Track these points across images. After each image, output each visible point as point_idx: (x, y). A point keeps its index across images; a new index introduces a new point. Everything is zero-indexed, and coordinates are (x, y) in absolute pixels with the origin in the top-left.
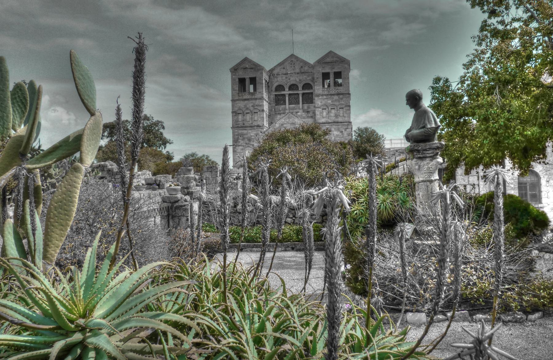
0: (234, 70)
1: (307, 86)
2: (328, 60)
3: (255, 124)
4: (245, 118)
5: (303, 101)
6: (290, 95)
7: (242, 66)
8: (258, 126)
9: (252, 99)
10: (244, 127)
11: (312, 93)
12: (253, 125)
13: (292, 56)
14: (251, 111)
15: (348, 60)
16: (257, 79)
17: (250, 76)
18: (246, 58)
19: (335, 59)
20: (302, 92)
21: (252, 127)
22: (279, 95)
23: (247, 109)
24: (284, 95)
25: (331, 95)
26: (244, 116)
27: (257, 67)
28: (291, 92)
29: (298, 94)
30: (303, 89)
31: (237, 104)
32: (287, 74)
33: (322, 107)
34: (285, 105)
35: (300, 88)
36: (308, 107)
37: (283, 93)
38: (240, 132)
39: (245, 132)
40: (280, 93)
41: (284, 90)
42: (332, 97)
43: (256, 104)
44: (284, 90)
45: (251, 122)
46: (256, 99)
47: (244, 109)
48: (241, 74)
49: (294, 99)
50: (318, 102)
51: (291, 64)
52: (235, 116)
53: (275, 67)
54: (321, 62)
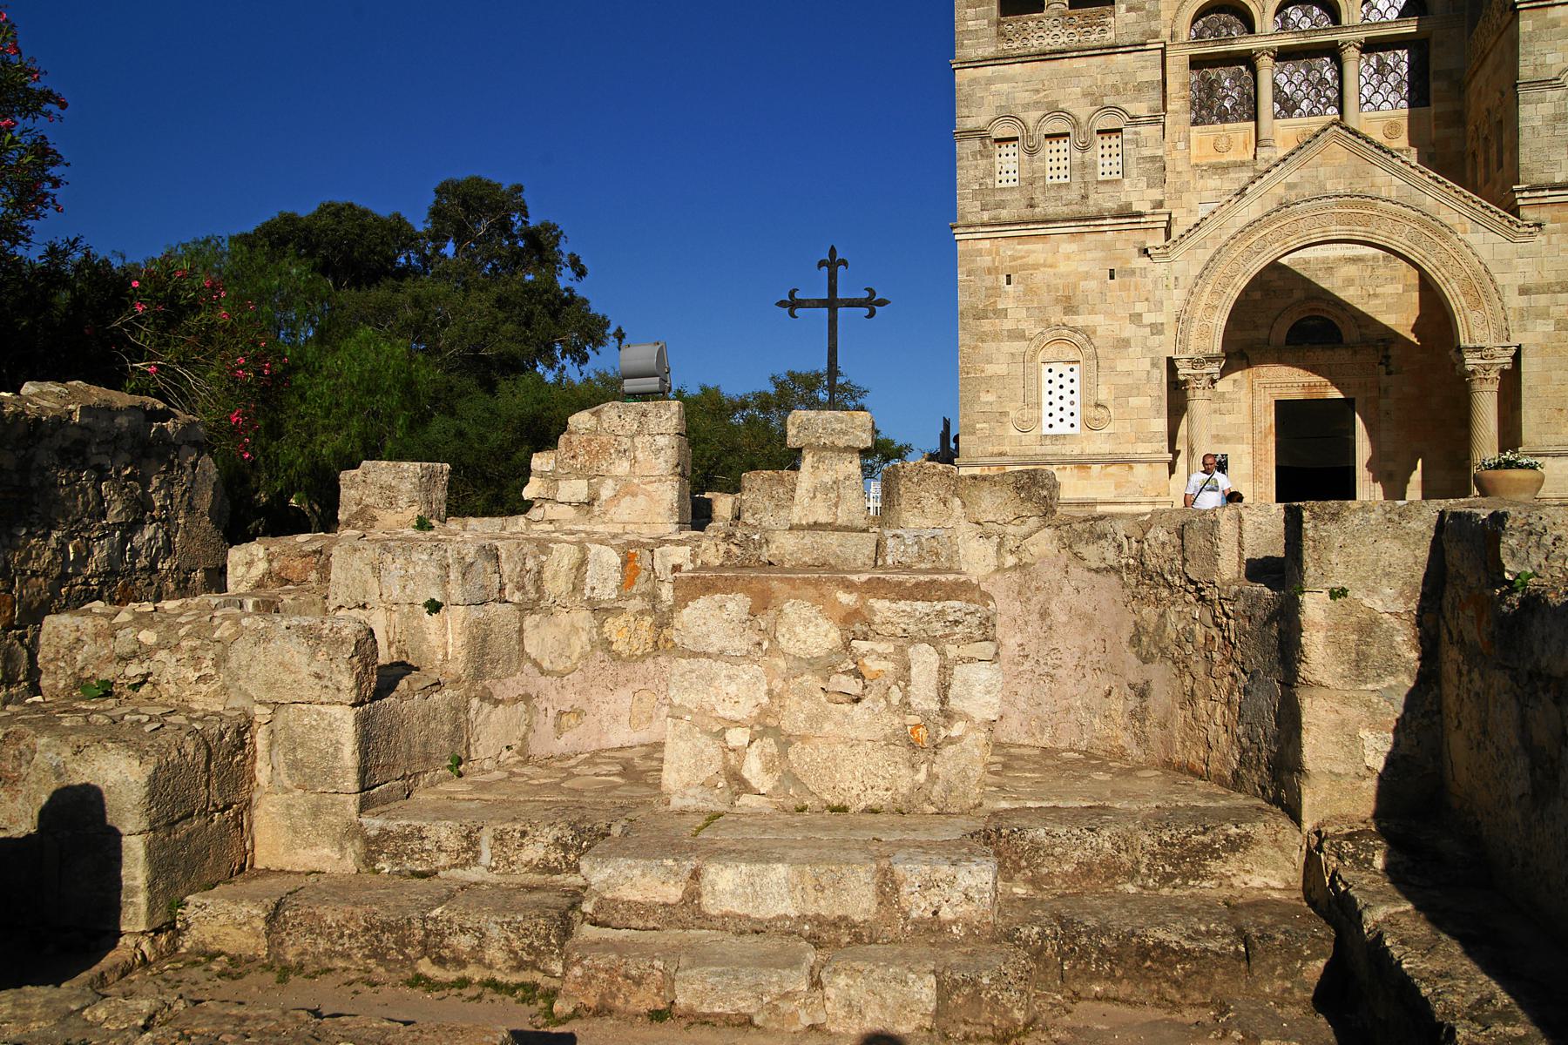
3: (1104, 200)
4: (1037, 164)
8: (1126, 213)
9: (1084, 52)
12: (1093, 210)
14: (1076, 124)
20: (1362, 35)
23: (1055, 111)
26: (1032, 152)
28: (1289, 40)
31: (990, 81)
34: (1255, 117)
37: (1243, 44)
38: (1009, 249)
39: (1036, 252)
40: (1221, 49)
43: (1110, 80)
44: (1250, 27)
45: (1074, 195)
46: (1112, 49)
47: (1031, 117)
52: (985, 154)
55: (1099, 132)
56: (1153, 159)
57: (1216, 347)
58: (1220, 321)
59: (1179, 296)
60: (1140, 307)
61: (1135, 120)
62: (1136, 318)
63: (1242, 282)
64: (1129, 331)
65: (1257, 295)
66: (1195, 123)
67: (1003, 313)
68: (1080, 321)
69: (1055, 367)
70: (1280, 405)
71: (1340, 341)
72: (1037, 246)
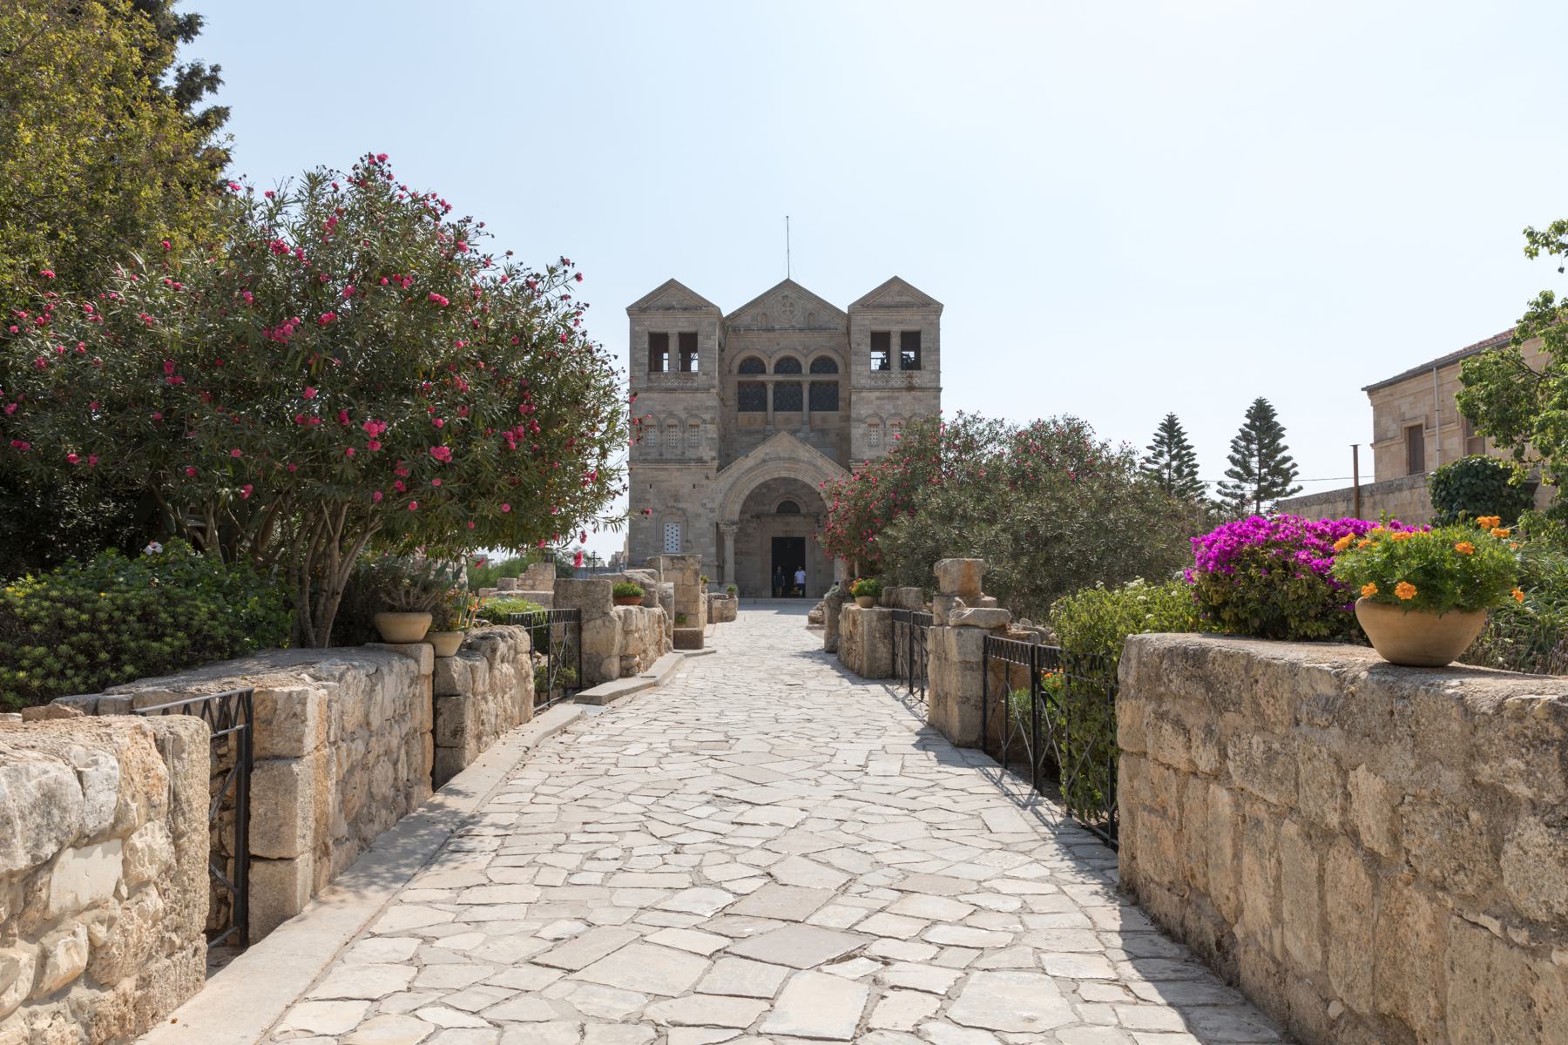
0: (637, 311)
1: (823, 364)
2: (888, 300)
3: (691, 454)
5: (811, 402)
6: (778, 384)
7: (659, 303)
8: (700, 460)
9: (682, 389)
10: (661, 460)
11: (836, 384)
13: (788, 283)
14: (681, 421)
15: (938, 303)
16: (700, 338)
17: (681, 330)
18: (672, 280)
19: (905, 299)
21: (682, 461)
22: (749, 384)
23: (671, 414)
24: (763, 385)
25: (892, 389)
27: (697, 305)
28: (780, 378)
29: (799, 384)
30: (812, 371)
32: (772, 330)
33: (869, 421)
35: (806, 369)
36: (824, 420)
37: (760, 378)
39: (663, 475)
40: (752, 379)
41: (763, 371)
42: (897, 394)
43: (695, 404)
44: (763, 371)
46: (696, 390)
47: (662, 416)
48: (660, 324)
49: (788, 399)
50: (864, 405)
51: (784, 305)
53: (741, 310)
54: (867, 304)
55: (691, 426)
56: (712, 439)
57: (736, 517)
58: (737, 508)
59: (721, 496)
60: (705, 501)
61: (704, 421)
62: (704, 505)
63: (747, 492)
64: (701, 510)
65: (765, 490)
66: (740, 410)
67: (648, 501)
68: (681, 505)
69: (671, 525)
70: (774, 539)
71: (799, 511)
72: (663, 473)
